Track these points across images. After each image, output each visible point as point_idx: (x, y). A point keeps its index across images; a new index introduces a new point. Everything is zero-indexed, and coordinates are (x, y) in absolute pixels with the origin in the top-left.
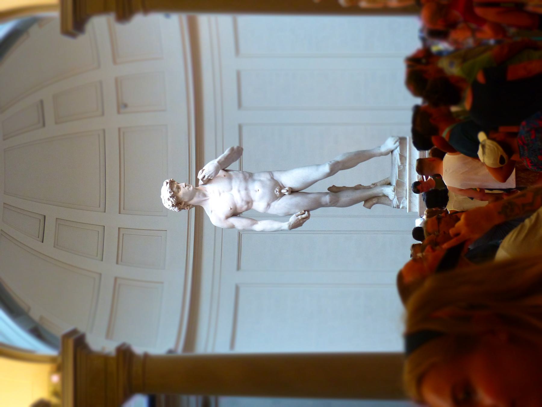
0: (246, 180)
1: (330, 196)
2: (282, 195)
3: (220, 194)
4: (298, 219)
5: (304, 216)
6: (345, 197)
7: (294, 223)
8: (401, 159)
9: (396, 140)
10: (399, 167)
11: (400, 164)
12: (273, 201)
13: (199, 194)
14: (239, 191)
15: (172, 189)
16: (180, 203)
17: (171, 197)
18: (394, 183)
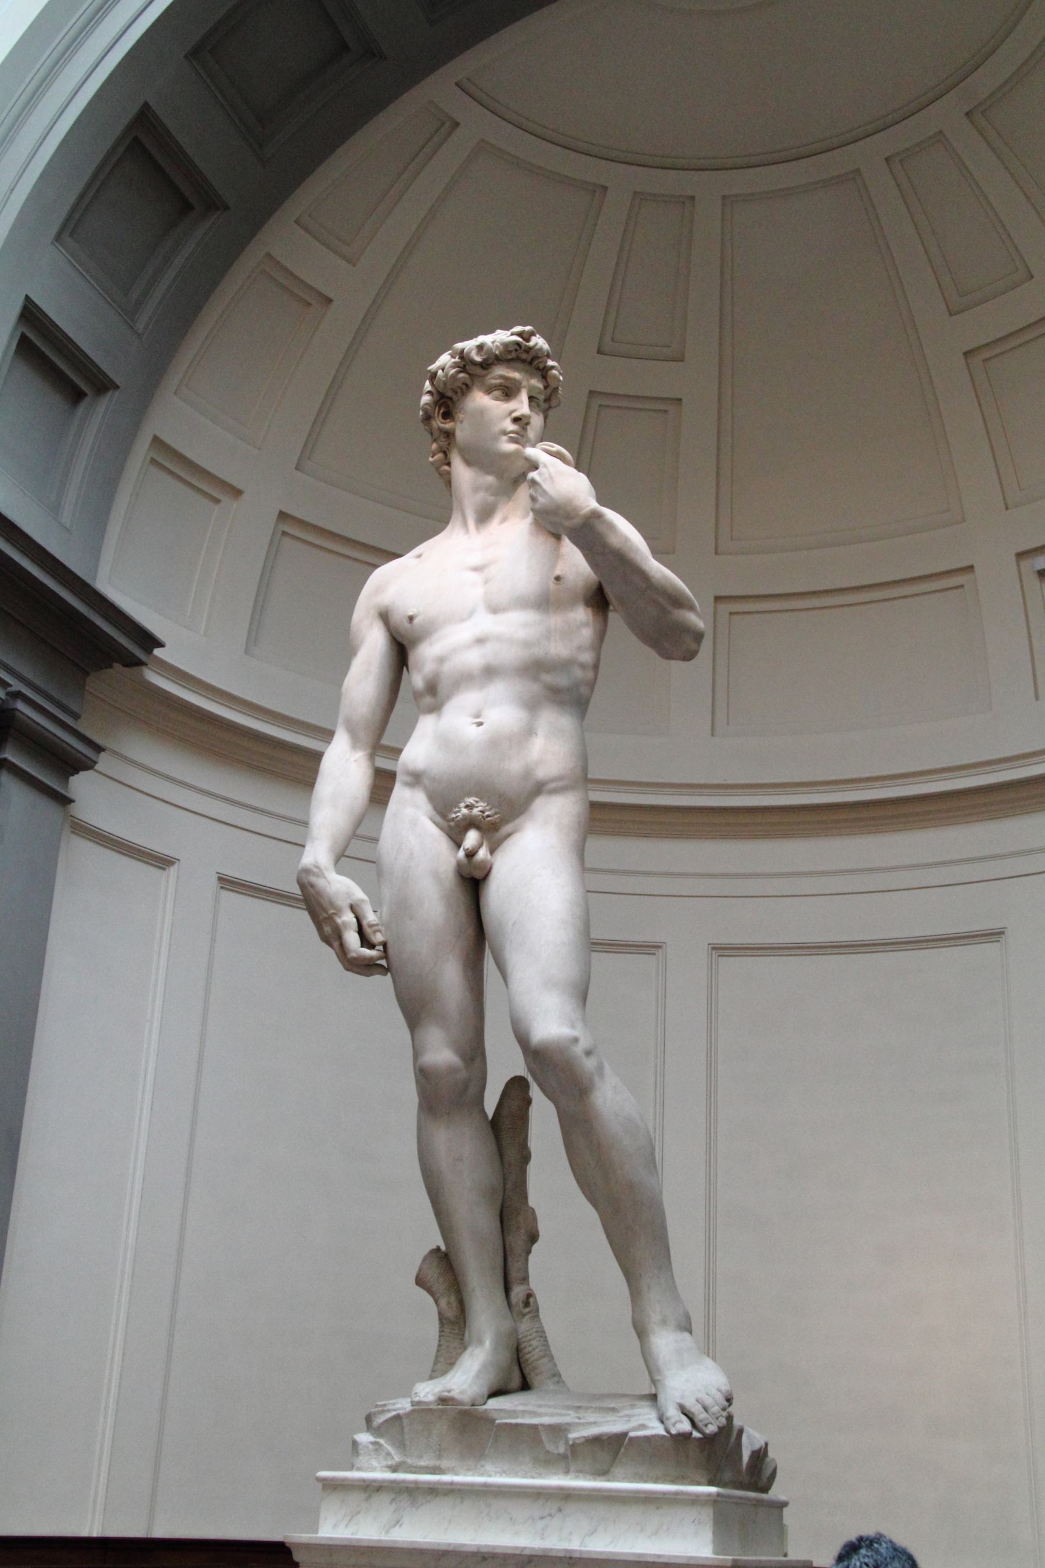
0: (534, 668)
1: (452, 1070)
2: (455, 834)
3: (476, 569)
4: (339, 911)
5: (352, 939)
6: (463, 1149)
7: (319, 893)
8: (597, 1441)
9: (701, 1416)
10: (558, 1431)
11: (572, 1436)
12: (432, 797)
13: (488, 488)
14: (480, 641)
15: (491, 360)
16: (448, 415)
17: (462, 354)
18: (494, 1404)
